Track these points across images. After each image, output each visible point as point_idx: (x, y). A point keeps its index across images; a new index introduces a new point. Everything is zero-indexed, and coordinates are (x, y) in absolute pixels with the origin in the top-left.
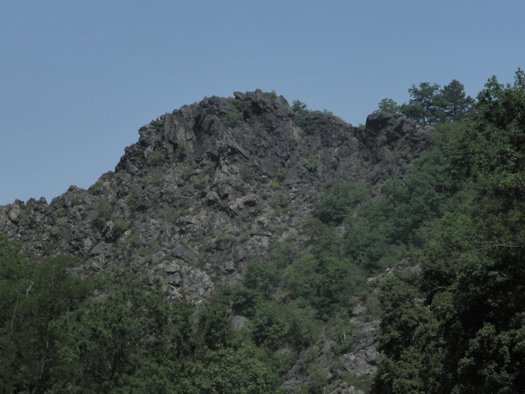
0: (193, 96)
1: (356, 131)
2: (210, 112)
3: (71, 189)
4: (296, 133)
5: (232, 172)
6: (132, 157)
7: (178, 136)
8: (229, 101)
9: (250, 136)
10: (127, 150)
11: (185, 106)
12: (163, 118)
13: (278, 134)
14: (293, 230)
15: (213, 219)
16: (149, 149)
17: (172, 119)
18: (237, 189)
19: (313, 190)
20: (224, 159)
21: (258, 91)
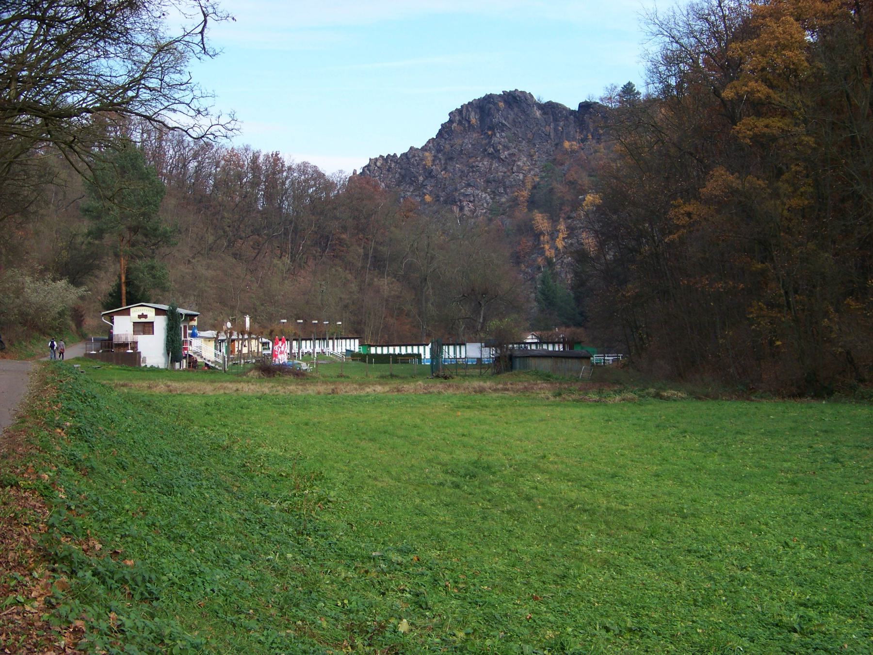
0: (479, 93)
2: (489, 102)
3: (411, 148)
4: (538, 114)
6: (445, 130)
9: (511, 116)
10: (442, 125)
13: (528, 115)
14: (537, 170)
15: (491, 165)
16: (455, 125)
18: (504, 146)
19: (549, 146)
21: (516, 90)
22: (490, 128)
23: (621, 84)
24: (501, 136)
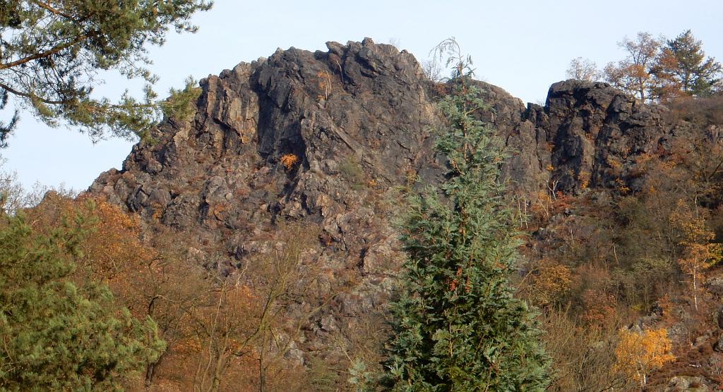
1: (530, 112)
5: (326, 170)
7: (232, 114)
8: (319, 56)
9: (355, 115)
11: (243, 65)
12: (205, 84)
17: (219, 85)
20: (314, 151)
21: (366, 42)
22: (288, 147)
23: (666, 32)
24: (326, 170)
